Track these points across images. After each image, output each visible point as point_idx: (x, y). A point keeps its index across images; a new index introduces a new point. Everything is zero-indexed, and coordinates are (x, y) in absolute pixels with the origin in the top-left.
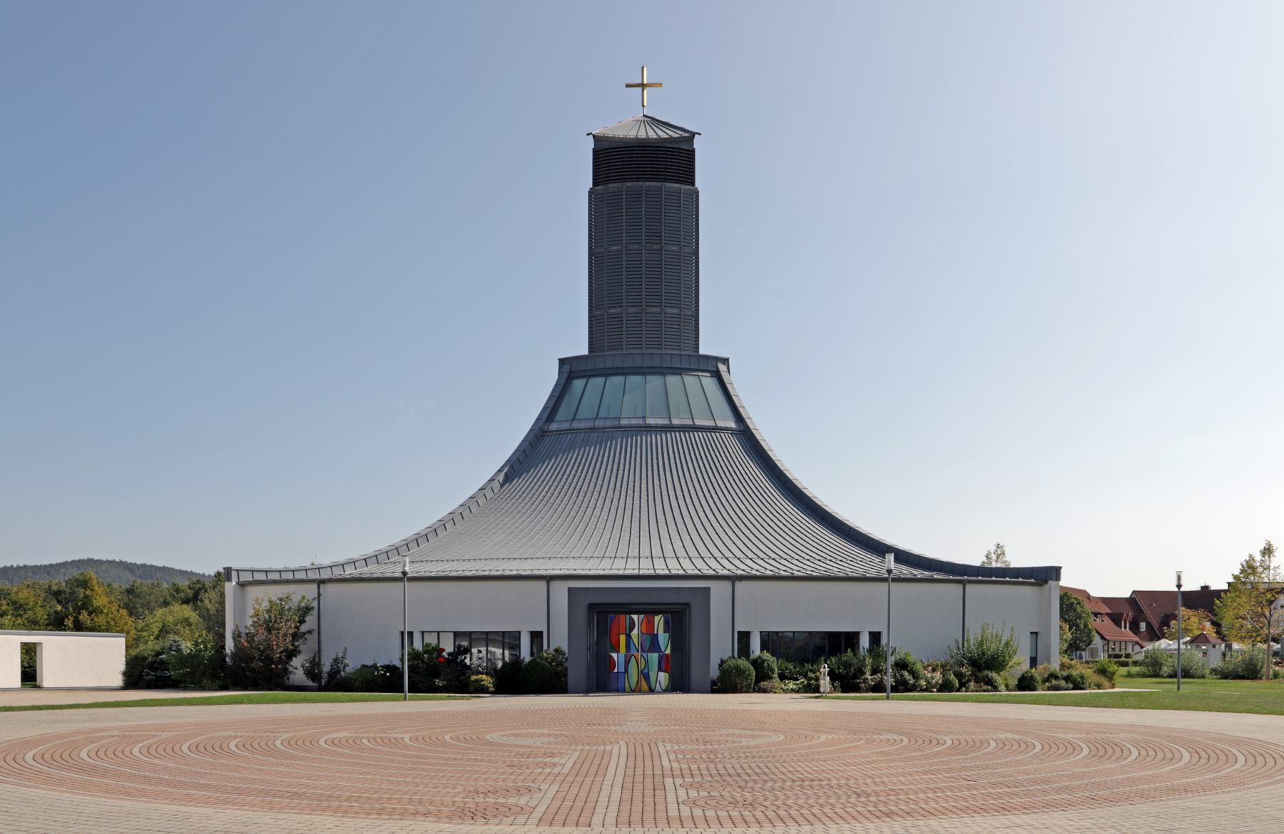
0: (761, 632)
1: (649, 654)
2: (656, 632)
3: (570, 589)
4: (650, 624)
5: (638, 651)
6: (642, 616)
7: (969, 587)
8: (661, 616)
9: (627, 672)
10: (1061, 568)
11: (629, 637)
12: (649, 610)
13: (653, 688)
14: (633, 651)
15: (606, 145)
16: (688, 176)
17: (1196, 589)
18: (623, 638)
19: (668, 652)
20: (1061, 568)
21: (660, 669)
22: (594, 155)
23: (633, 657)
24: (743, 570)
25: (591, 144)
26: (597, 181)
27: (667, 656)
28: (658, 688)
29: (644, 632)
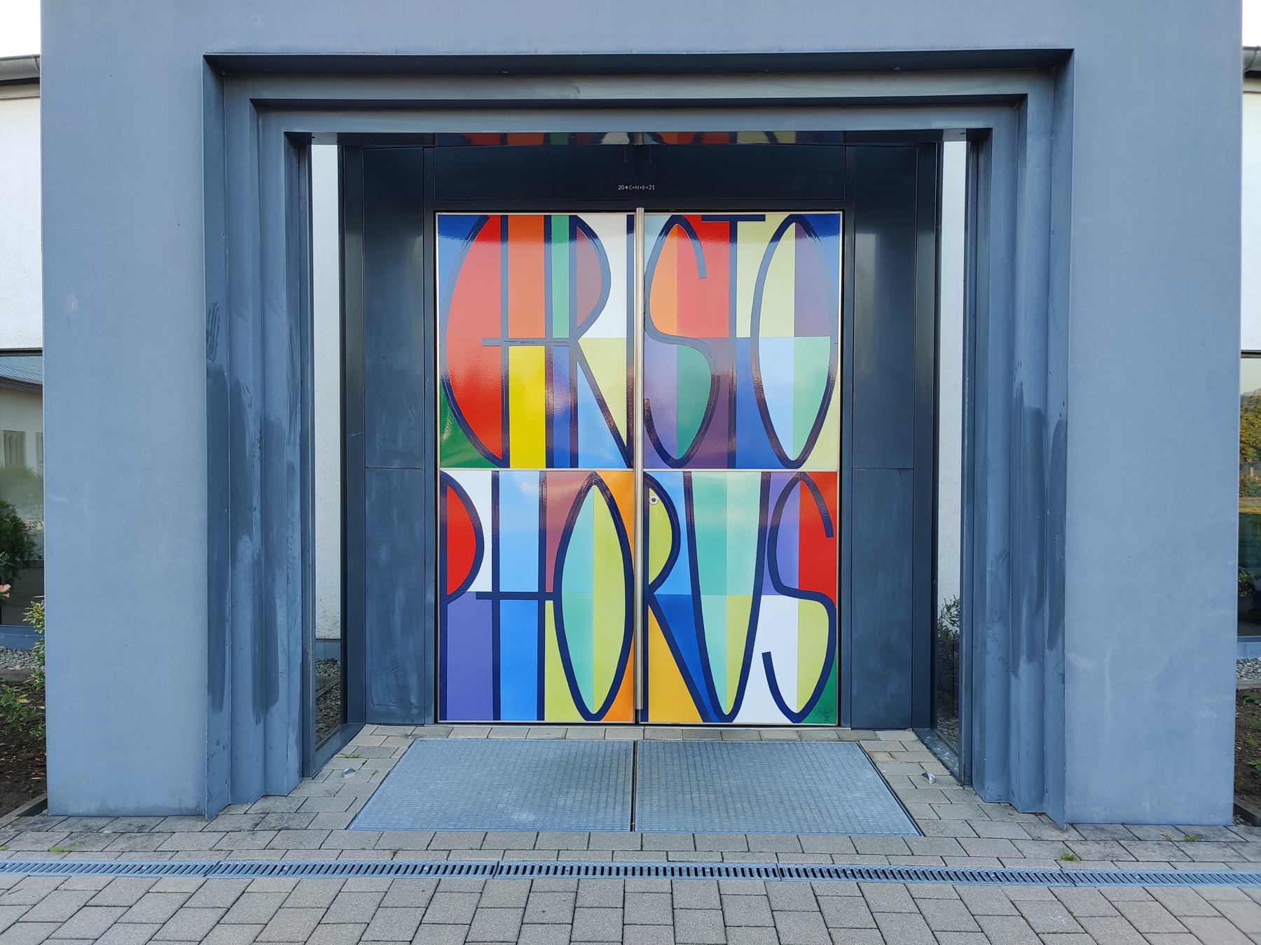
1: (699, 475)
2: (743, 330)
5: (629, 461)
9: (557, 597)
13: (727, 708)
19: (825, 458)
29: (667, 323)
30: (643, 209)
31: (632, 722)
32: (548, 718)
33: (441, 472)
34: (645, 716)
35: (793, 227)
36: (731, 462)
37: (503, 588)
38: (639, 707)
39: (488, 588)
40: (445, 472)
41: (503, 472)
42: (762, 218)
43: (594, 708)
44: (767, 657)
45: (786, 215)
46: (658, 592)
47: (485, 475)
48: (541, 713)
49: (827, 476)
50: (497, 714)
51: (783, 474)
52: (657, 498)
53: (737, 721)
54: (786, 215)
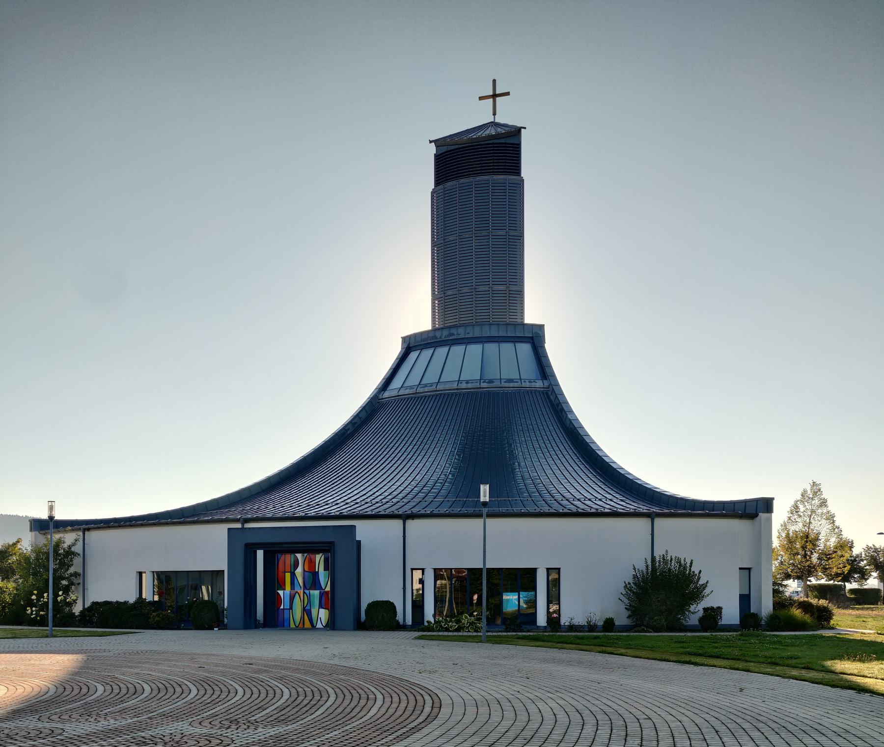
0: (435, 569)
1: (311, 591)
2: (317, 570)
3: (229, 529)
4: (312, 563)
6: (306, 555)
7: (659, 522)
8: (321, 554)
10: (773, 499)
11: (293, 575)
12: (309, 549)
14: (297, 589)
15: (444, 149)
16: (514, 166)
17: (45, 518)
18: (288, 576)
19: (328, 589)
20: (773, 499)
21: (321, 606)
22: (436, 159)
24: (583, 509)
25: (432, 149)
26: (438, 182)
27: (327, 593)
28: (319, 626)
43: (297, 626)
47: (282, 591)
50: (284, 626)
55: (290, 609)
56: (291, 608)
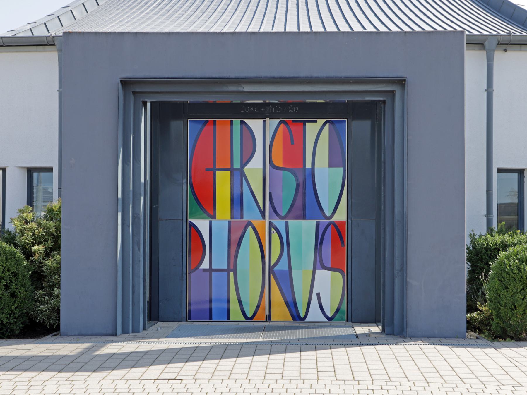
2: (308, 165)
8: (321, 122)
13: (302, 315)
19: (341, 216)
23: (250, 228)
27: (338, 228)
29: (279, 163)
30: (269, 118)
31: (265, 321)
32: (231, 319)
33: (189, 221)
34: (270, 319)
35: (328, 125)
36: (303, 217)
37: (213, 267)
38: (268, 313)
39: (207, 267)
40: (191, 221)
41: (213, 221)
42: (316, 121)
43: (249, 315)
44: (318, 295)
45: (325, 120)
46: (275, 269)
47: (207, 222)
48: (228, 318)
49: (342, 223)
50: (211, 318)
51: (324, 222)
52: (274, 231)
53: (306, 320)
54: (325, 120)
55: (228, 271)
56: (232, 268)
